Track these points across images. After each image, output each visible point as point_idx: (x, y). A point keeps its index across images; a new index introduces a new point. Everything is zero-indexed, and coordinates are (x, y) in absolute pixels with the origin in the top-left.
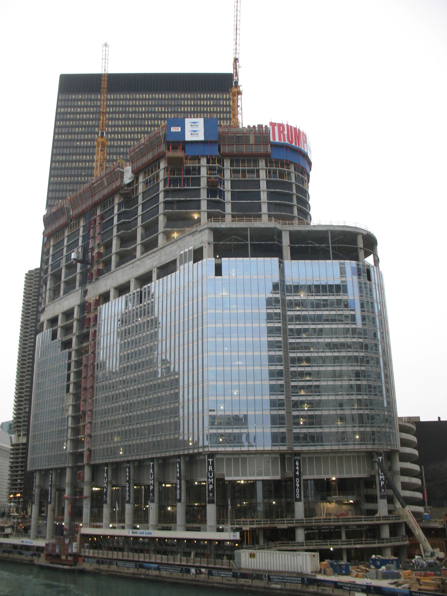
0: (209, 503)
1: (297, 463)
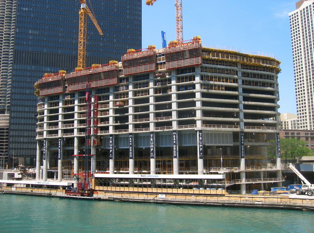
0: (200, 158)
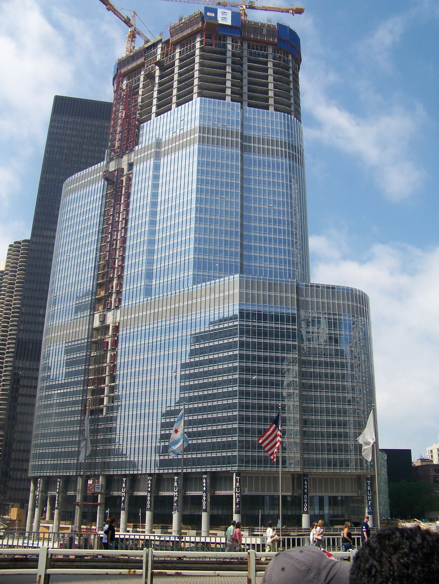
0: (235, 513)
1: (306, 483)
